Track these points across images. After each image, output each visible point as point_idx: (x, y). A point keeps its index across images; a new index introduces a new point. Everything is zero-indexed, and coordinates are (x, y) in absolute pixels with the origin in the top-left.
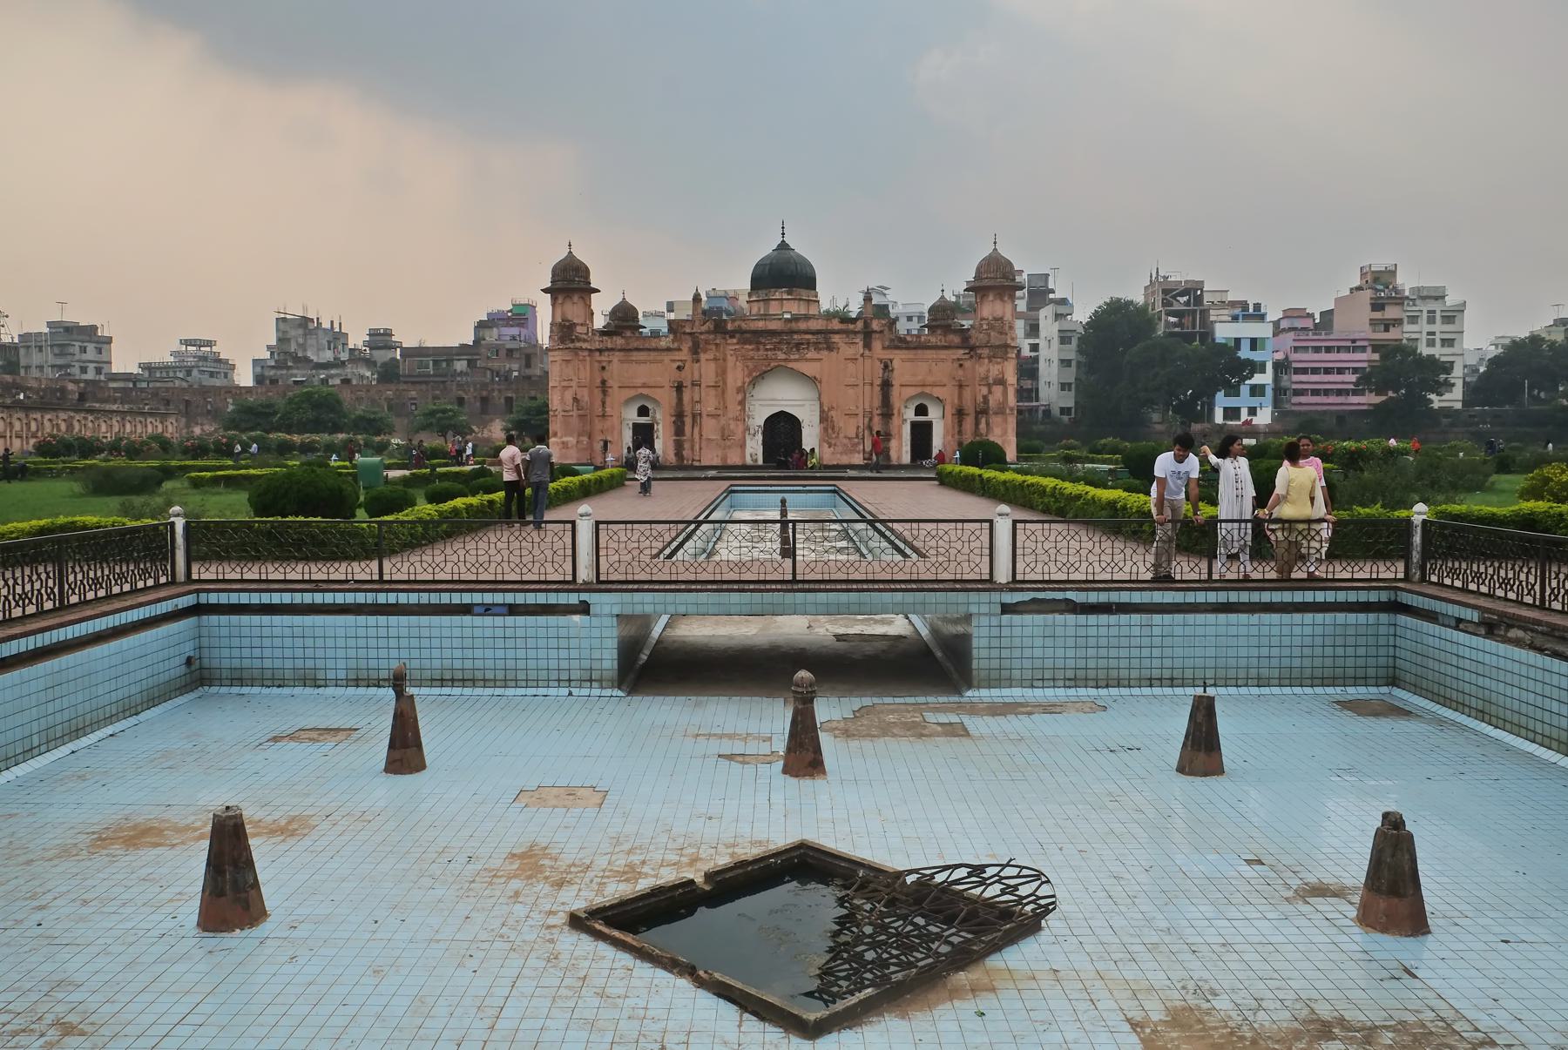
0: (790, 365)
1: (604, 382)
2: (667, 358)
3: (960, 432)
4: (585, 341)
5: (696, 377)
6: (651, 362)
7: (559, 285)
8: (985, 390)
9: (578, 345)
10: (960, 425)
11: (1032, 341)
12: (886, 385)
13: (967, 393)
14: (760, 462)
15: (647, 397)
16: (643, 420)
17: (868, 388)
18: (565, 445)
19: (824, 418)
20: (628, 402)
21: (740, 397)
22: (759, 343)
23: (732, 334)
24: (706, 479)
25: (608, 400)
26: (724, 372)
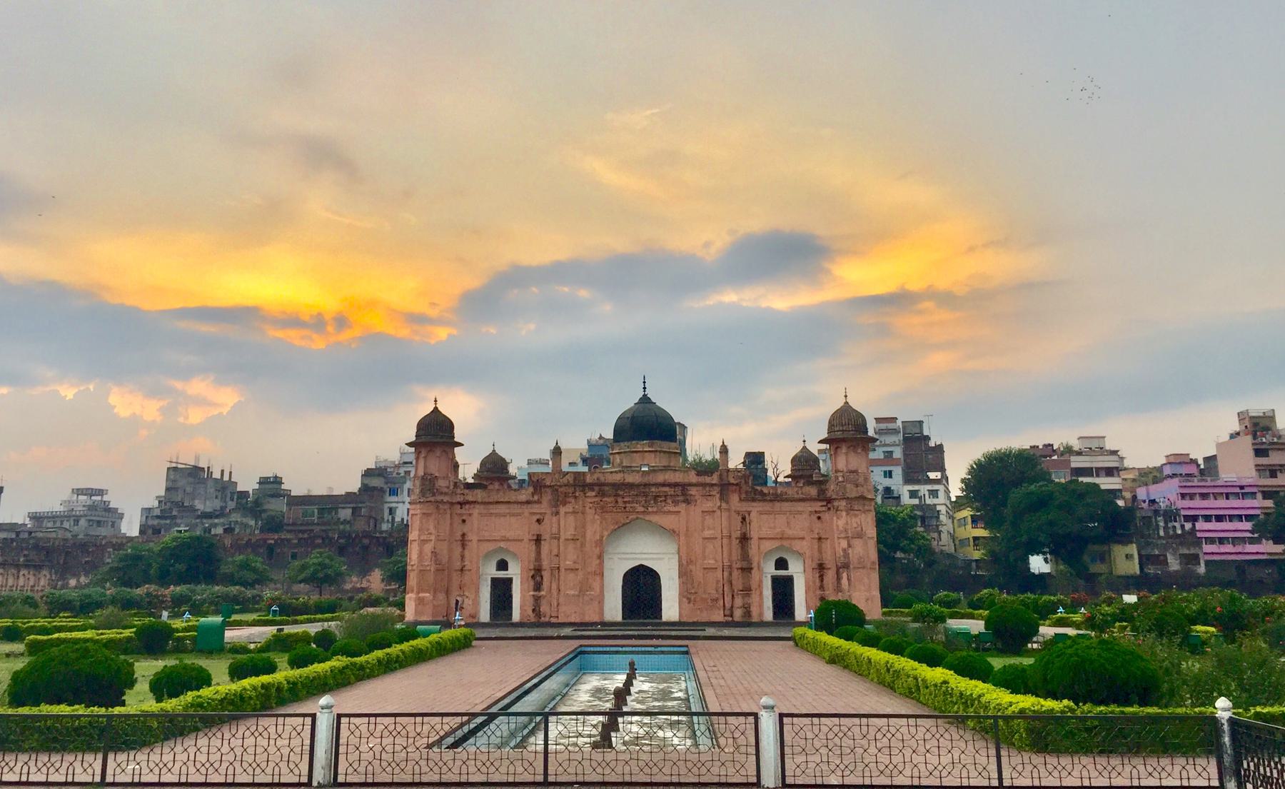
0: (647, 518)
1: (464, 535)
2: (526, 510)
3: (822, 587)
4: (446, 494)
5: (555, 530)
6: (514, 515)
7: (423, 439)
8: (844, 544)
9: (439, 498)
10: (821, 577)
11: (911, 488)
12: (744, 539)
13: (827, 546)
14: (618, 617)
15: (507, 551)
16: (502, 574)
17: (725, 541)
18: (420, 602)
19: (684, 573)
20: (488, 556)
21: (597, 551)
22: (617, 495)
23: (591, 486)
24: (559, 638)
25: (467, 553)
26: (584, 527)
